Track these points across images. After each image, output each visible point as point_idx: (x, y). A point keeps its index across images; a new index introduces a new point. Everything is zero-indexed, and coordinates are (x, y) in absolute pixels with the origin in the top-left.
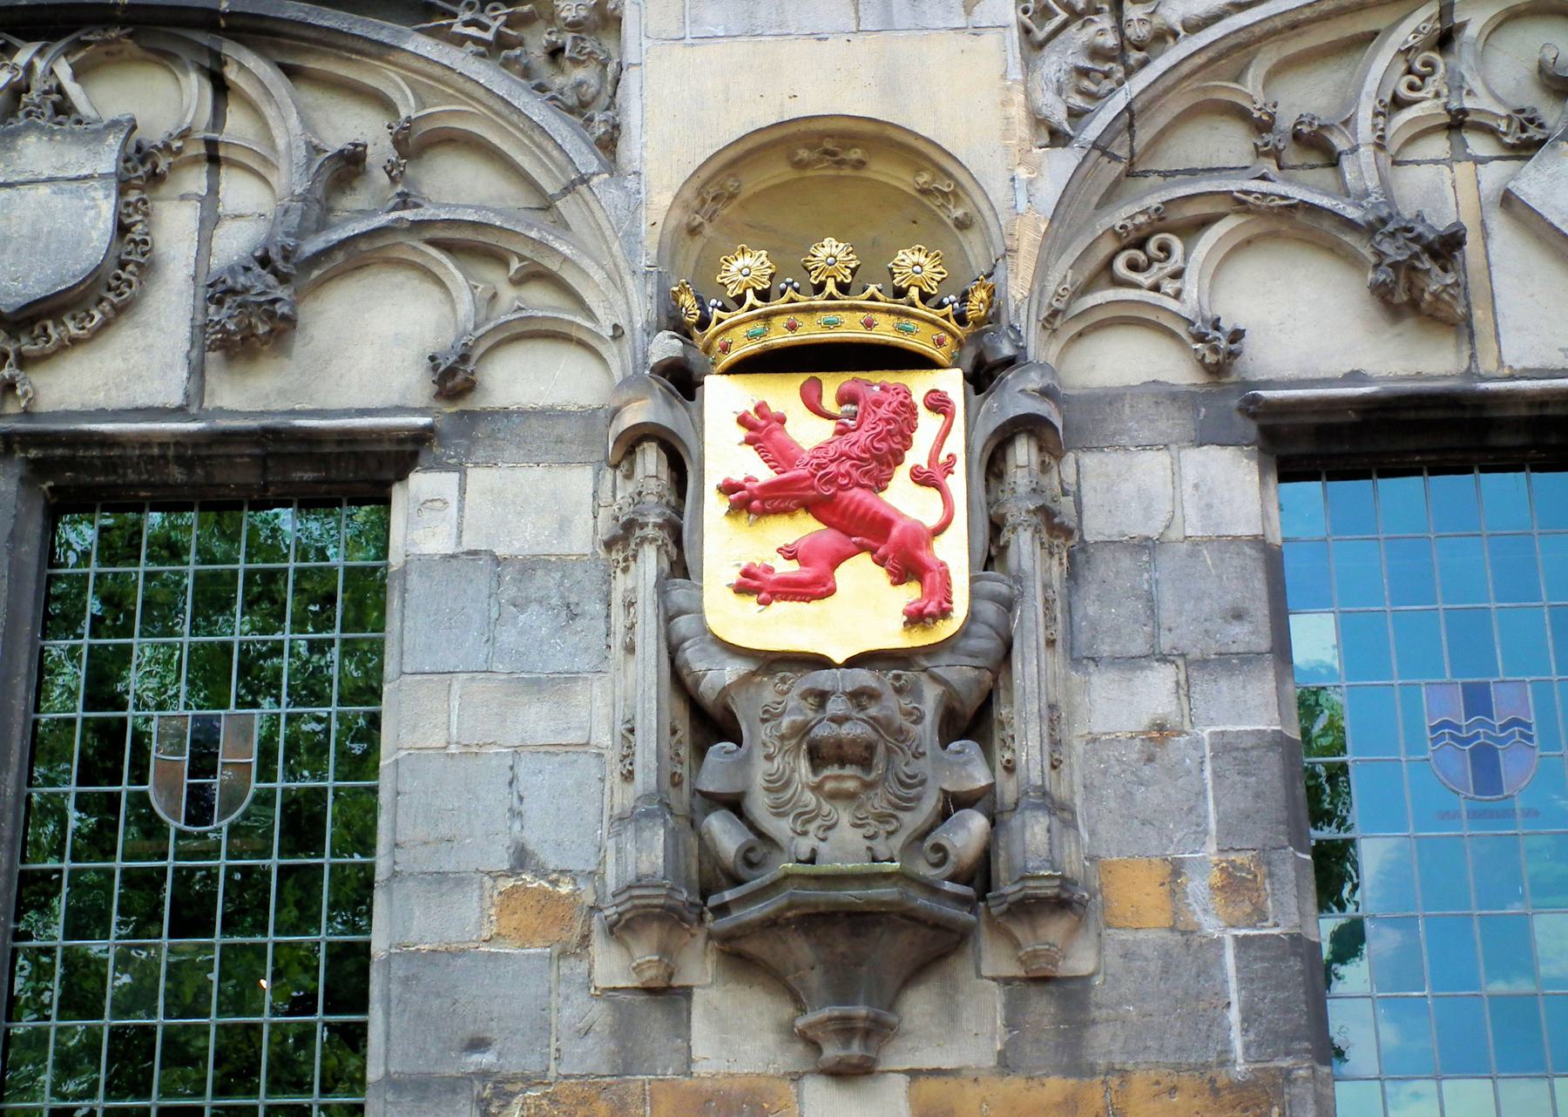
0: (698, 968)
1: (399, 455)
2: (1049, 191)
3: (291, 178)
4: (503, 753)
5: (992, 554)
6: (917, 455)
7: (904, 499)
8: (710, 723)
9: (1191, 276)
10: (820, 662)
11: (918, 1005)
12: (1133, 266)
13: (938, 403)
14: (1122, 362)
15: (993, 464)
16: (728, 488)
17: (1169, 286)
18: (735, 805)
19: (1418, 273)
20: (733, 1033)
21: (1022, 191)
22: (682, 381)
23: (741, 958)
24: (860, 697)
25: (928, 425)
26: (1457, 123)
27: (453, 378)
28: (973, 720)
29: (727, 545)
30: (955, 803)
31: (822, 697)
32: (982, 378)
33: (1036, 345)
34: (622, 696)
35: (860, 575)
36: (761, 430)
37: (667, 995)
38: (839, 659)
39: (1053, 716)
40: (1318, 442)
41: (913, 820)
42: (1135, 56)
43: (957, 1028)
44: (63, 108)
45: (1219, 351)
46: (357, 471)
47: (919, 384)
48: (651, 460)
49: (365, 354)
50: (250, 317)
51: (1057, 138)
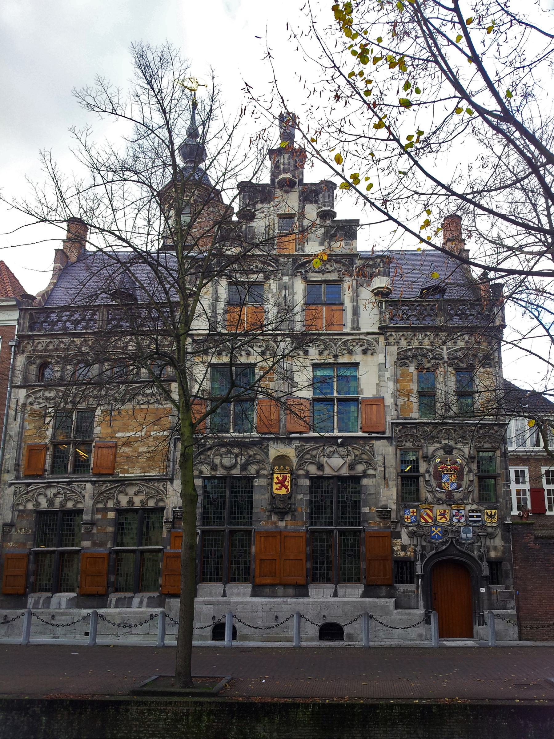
0: (273, 514)
1: (254, 478)
3: (247, 457)
4: (260, 499)
5: (291, 487)
7: (286, 483)
8: (274, 498)
11: (286, 516)
14: (301, 472)
15: (292, 480)
18: (275, 504)
19: (320, 467)
20: (274, 518)
21: (295, 461)
22: (272, 474)
23: (275, 513)
27: (258, 472)
28: (290, 498)
29: (275, 486)
32: (291, 475)
33: (295, 472)
34: (267, 496)
35: (283, 488)
36: (277, 478)
37: (271, 515)
39: (295, 498)
40: (312, 479)
43: (288, 518)
45: (307, 472)
46: (250, 479)
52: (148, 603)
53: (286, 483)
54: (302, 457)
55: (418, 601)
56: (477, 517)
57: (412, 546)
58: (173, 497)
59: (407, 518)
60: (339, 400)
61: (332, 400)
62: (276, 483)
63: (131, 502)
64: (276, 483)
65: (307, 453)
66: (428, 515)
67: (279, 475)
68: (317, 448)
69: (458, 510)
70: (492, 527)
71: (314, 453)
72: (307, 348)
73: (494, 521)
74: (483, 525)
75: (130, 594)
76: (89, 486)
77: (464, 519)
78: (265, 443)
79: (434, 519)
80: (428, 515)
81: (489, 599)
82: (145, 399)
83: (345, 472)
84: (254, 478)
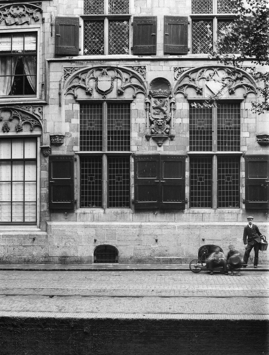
2: (175, 84)
6: (165, 105)
7: (164, 108)
9: (184, 90)
10: (159, 119)
12: (181, 89)
13: (167, 101)
16: (153, 107)
17: (183, 90)
24: (161, 122)
25: (166, 102)
26: (204, 78)
30: (167, 129)
31: (158, 122)
35: (161, 113)
36: (155, 102)
38: (160, 119)
41: (164, 130)
42: (182, 73)
44: (107, 74)
46: (128, 103)
47: (166, 99)
48: (148, 104)
49: (128, 95)
50: (120, 93)
51: (176, 80)
54: (181, 81)
60: (221, 19)
62: (154, 108)
65: (186, 76)
67: (157, 100)
68: (196, 70)
71: (193, 76)
82: (17, 20)
83: (225, 96)
84: (131, 101)
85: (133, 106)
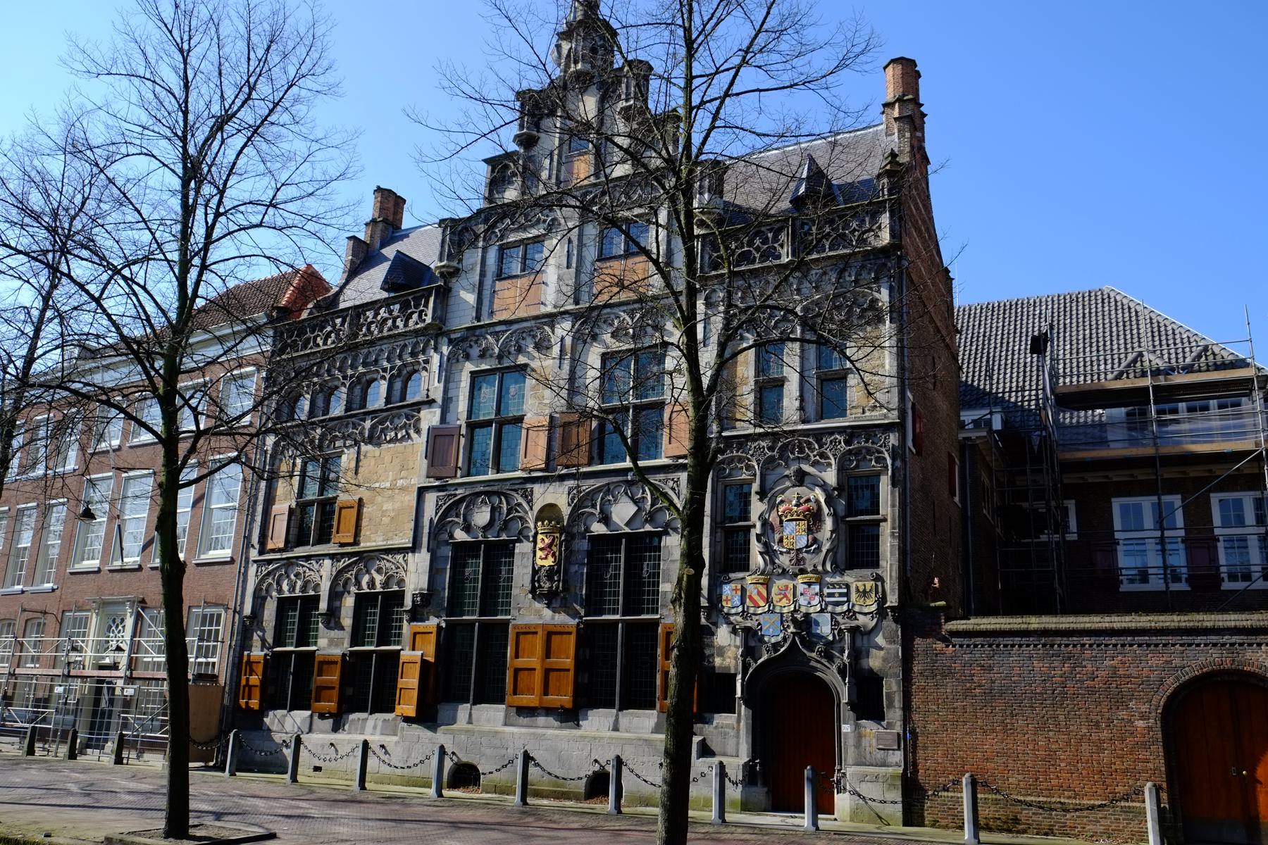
29: (539, 554)
52: (382, 728)
53: (554, 549)
55: (738, 743)
56: (841, 595)
57: (733, 649)
58: (415, 574)
59: (727, 600)
60: (635, 407)
61: (626, 409)
62: (541, 549)
63: (372, 583)
64: (541, 549)
66: (759, 594)
69: (809, 584)
70: (865, 614)
72: (597, 330)
73: (869, 602)
74: (849, 610)
75: (364, 715)
76: (327, 562)
77: (817, 599)
78: (529, 486)
79: (768, 600)
80: (759, 594)
81: (858, 745)
85: (519, 548)
